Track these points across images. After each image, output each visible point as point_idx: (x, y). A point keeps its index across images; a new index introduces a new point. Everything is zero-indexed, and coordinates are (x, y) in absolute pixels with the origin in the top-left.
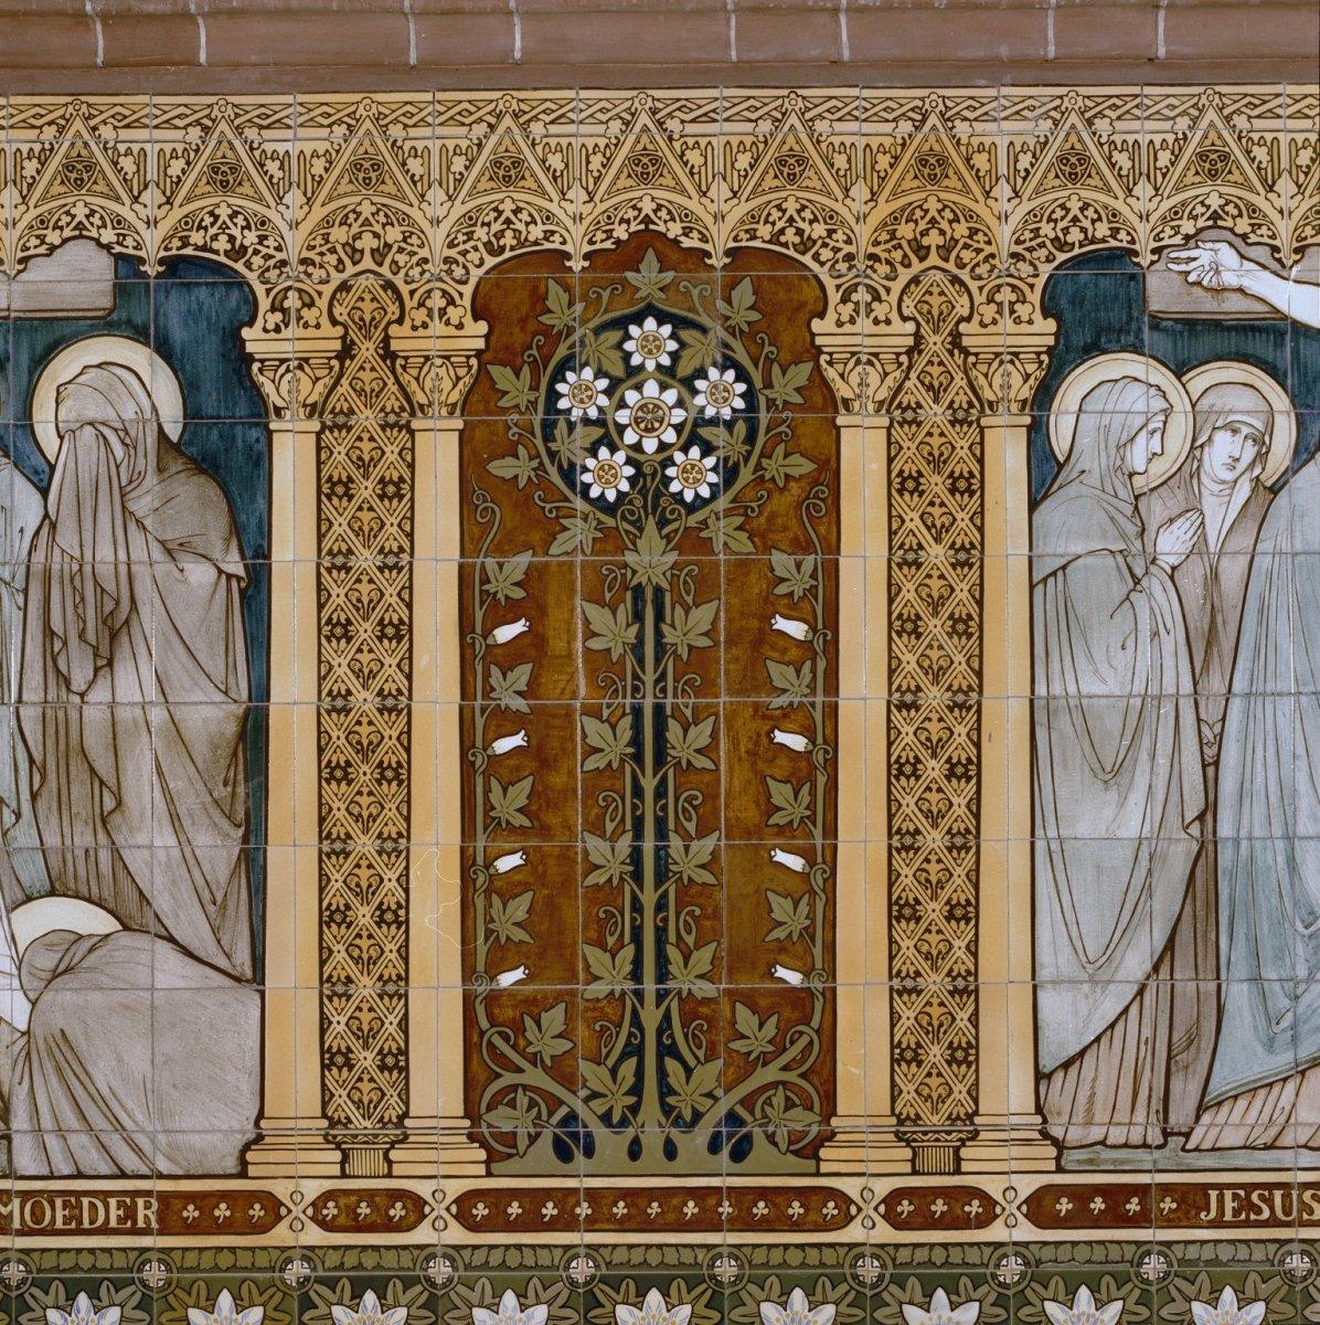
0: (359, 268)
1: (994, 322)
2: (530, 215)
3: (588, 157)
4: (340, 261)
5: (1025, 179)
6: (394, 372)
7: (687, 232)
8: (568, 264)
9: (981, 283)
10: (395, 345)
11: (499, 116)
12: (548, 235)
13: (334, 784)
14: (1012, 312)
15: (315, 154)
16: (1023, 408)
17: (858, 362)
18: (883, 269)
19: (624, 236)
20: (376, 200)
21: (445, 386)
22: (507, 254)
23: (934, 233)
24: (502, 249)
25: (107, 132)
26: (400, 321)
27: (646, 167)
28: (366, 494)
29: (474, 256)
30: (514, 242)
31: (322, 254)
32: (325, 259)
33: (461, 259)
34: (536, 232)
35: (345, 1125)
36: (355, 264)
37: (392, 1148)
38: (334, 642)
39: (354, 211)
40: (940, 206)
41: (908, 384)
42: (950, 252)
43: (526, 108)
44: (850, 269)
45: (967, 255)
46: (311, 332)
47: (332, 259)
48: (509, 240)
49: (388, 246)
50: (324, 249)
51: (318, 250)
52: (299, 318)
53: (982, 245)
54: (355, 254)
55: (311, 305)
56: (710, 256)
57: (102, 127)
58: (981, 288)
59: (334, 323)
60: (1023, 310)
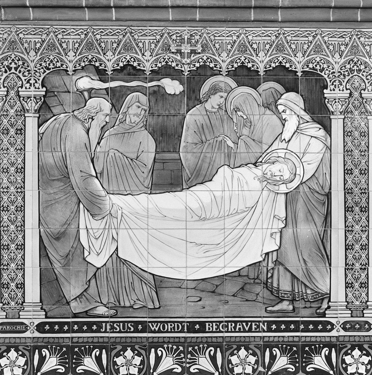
0: (11, 72)
1: (30, 88)
2: (57, 59)
3: (36, 43)
4: (6, 70)
5: (115, 50)
6: (20, 101)
7: (139, 65)
8: (107, 72)
9: (26, 78)
10: (20, 93)
11: (126, 33)
12: (62, 65)
13: (4, 212)
14: (34, 86)
15: (305, 43)
16: (36, 111)
17: (31, 100)
18: (38, 74)
19: (160, 66)
20: (92, 54)
21: (32, 105)
22: (51, 70)
23: (13, 63)
24: (50, 69)
25: (250, 38)
26: (22, 87)
27: (128, 48)
28: (12, 133)
29: (42, 70)
30: (53, 67)
31: (39, 69)
32: (40, 71)
33: (38, 71)
34: (59, 64)
35: (8, 304)
36: (10, 71)
37: (20, 311)
38: (4, 173)
39: (10, 57)
40: (15, 56)
41: (350, 106)
42: (17, 69)
43: (57, 31)
44: (29, 74)
45: (22, 70)
46: (37, 90)
47: (42, 70)
48: (51, 66)
49: (19, 66)
50: (40, 68)
51: (38, 68)
52: (34, 86)
53: (26, 67)
54: (10, 69)
55: (36, 82)
56: (107, 71)
57: (249, 36)
58: (25, 80)
59: (4, 87)
60: (37, 85)
